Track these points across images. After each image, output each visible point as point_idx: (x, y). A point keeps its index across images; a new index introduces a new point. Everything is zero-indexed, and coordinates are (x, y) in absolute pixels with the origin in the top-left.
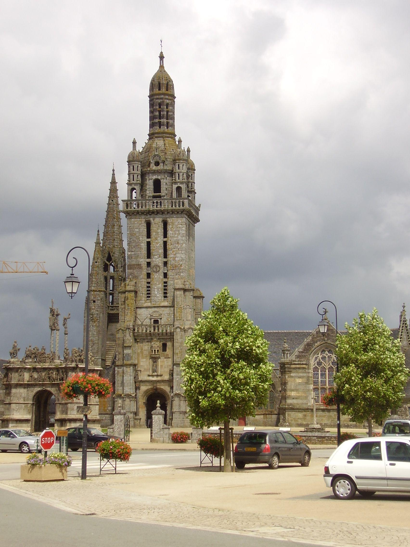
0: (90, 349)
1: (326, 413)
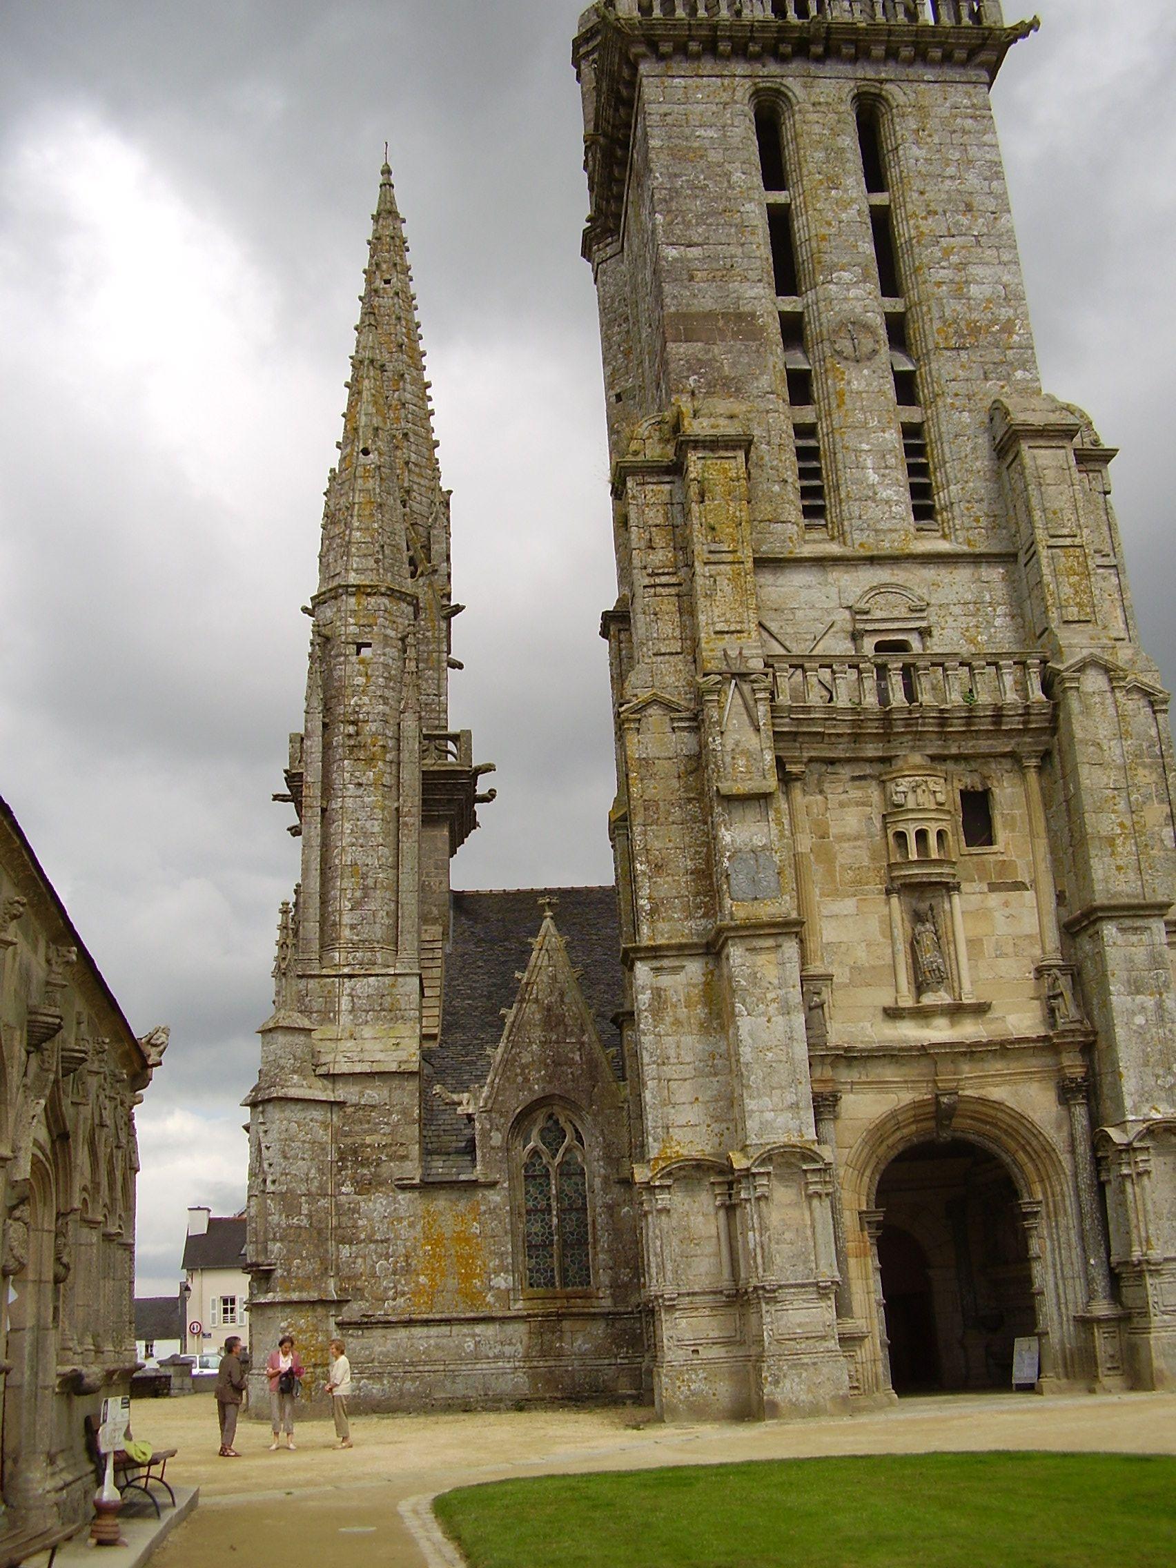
0: (347, 919)
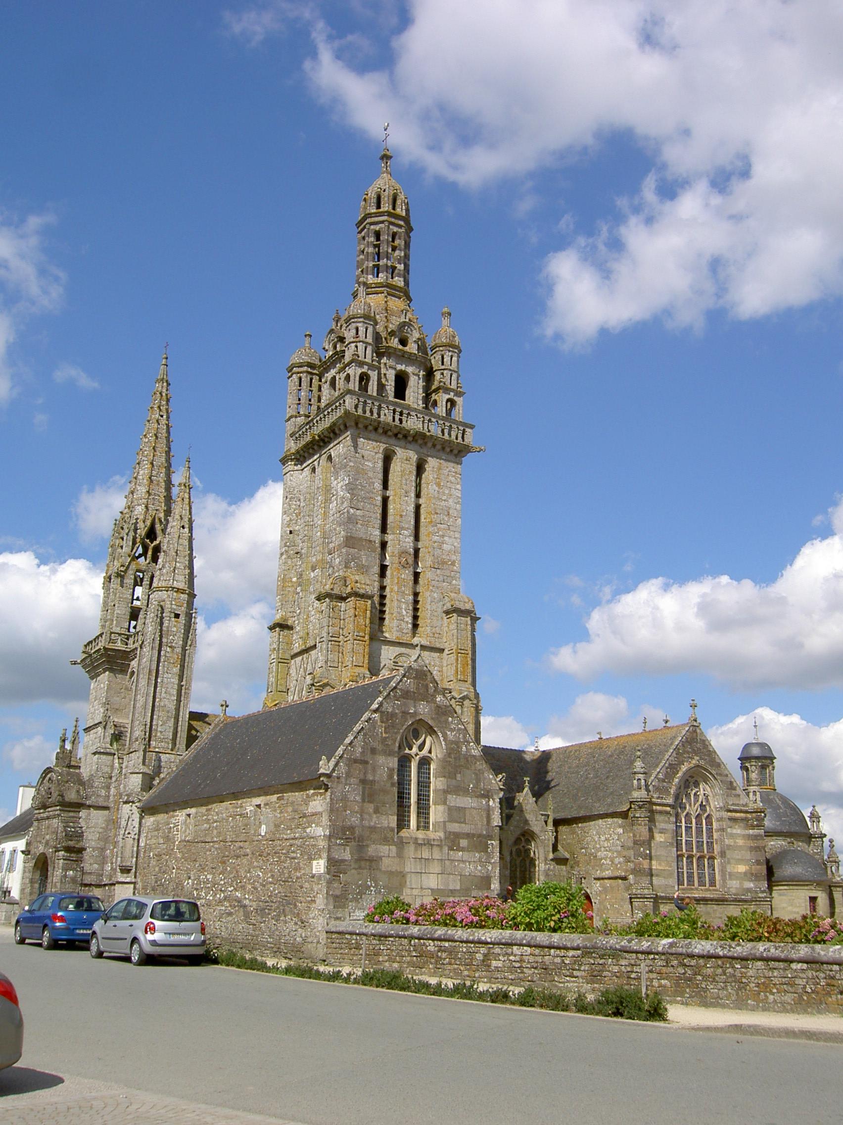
0: (159, 729)
1: (702, 906)
